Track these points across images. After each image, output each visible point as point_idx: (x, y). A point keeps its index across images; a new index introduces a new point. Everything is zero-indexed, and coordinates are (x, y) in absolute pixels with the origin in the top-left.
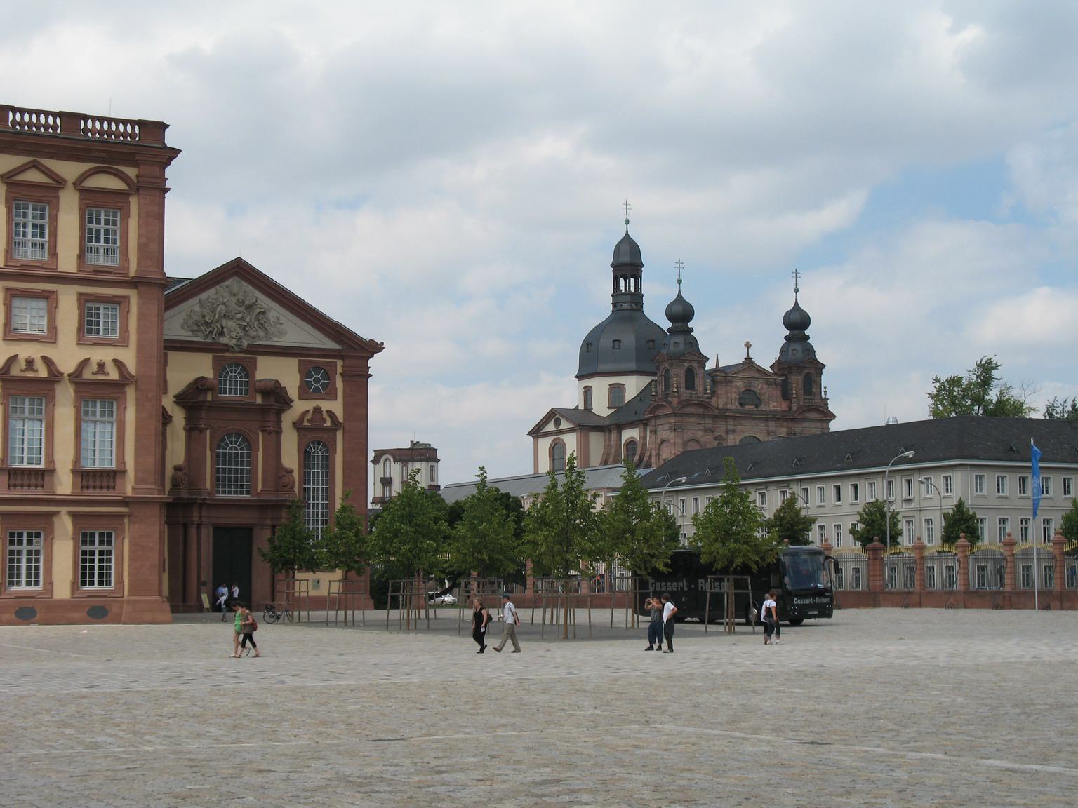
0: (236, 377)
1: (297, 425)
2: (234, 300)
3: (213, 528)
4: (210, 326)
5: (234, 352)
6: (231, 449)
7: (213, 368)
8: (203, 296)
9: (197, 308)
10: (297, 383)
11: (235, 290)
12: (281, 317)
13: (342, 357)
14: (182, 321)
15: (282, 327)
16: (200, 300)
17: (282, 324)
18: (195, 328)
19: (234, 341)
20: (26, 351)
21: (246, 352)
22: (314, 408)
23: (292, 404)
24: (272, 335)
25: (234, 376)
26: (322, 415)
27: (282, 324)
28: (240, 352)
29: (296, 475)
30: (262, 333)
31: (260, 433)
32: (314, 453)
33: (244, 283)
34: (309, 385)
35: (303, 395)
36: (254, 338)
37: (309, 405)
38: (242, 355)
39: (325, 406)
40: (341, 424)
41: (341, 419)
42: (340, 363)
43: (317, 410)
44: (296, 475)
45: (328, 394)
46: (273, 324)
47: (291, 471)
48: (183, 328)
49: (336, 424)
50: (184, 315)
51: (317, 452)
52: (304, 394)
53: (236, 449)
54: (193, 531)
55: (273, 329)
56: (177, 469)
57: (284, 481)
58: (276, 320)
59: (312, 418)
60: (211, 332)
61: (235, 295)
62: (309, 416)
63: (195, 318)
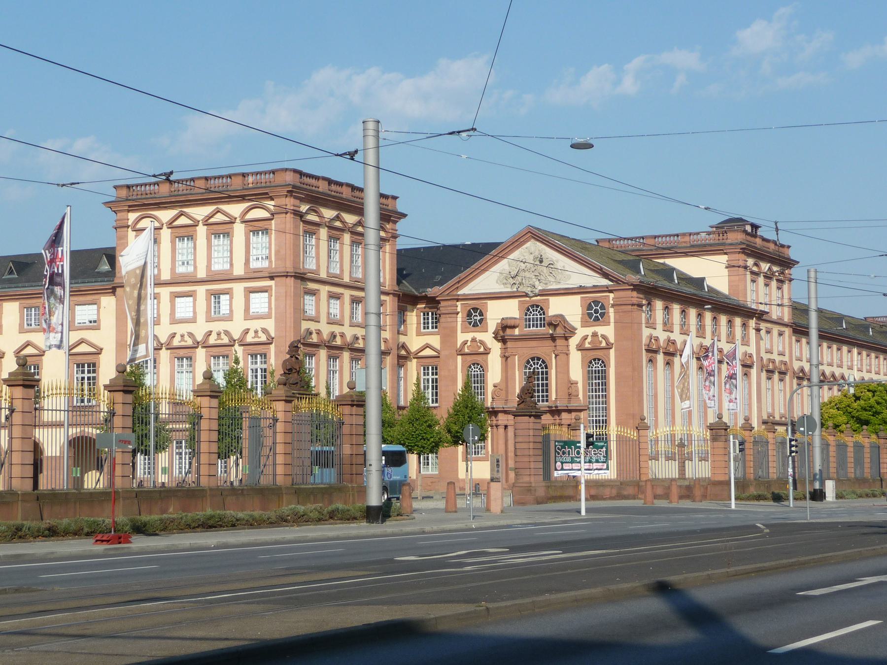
1: (580, 348)
2: (532, 257)
9: (507, 267)
11: (533, 249)
13: (611, 291)
19: (529, 289)
20: (181, 329)
25: (535, 315)
29: (580, 385)
30: (552, 279)
35: (584, 324)
37: (589, 331)
38: (539, 298)
41: (612, 340)
42: (612, 295)
43: (595, 335)
44: (580, 385)
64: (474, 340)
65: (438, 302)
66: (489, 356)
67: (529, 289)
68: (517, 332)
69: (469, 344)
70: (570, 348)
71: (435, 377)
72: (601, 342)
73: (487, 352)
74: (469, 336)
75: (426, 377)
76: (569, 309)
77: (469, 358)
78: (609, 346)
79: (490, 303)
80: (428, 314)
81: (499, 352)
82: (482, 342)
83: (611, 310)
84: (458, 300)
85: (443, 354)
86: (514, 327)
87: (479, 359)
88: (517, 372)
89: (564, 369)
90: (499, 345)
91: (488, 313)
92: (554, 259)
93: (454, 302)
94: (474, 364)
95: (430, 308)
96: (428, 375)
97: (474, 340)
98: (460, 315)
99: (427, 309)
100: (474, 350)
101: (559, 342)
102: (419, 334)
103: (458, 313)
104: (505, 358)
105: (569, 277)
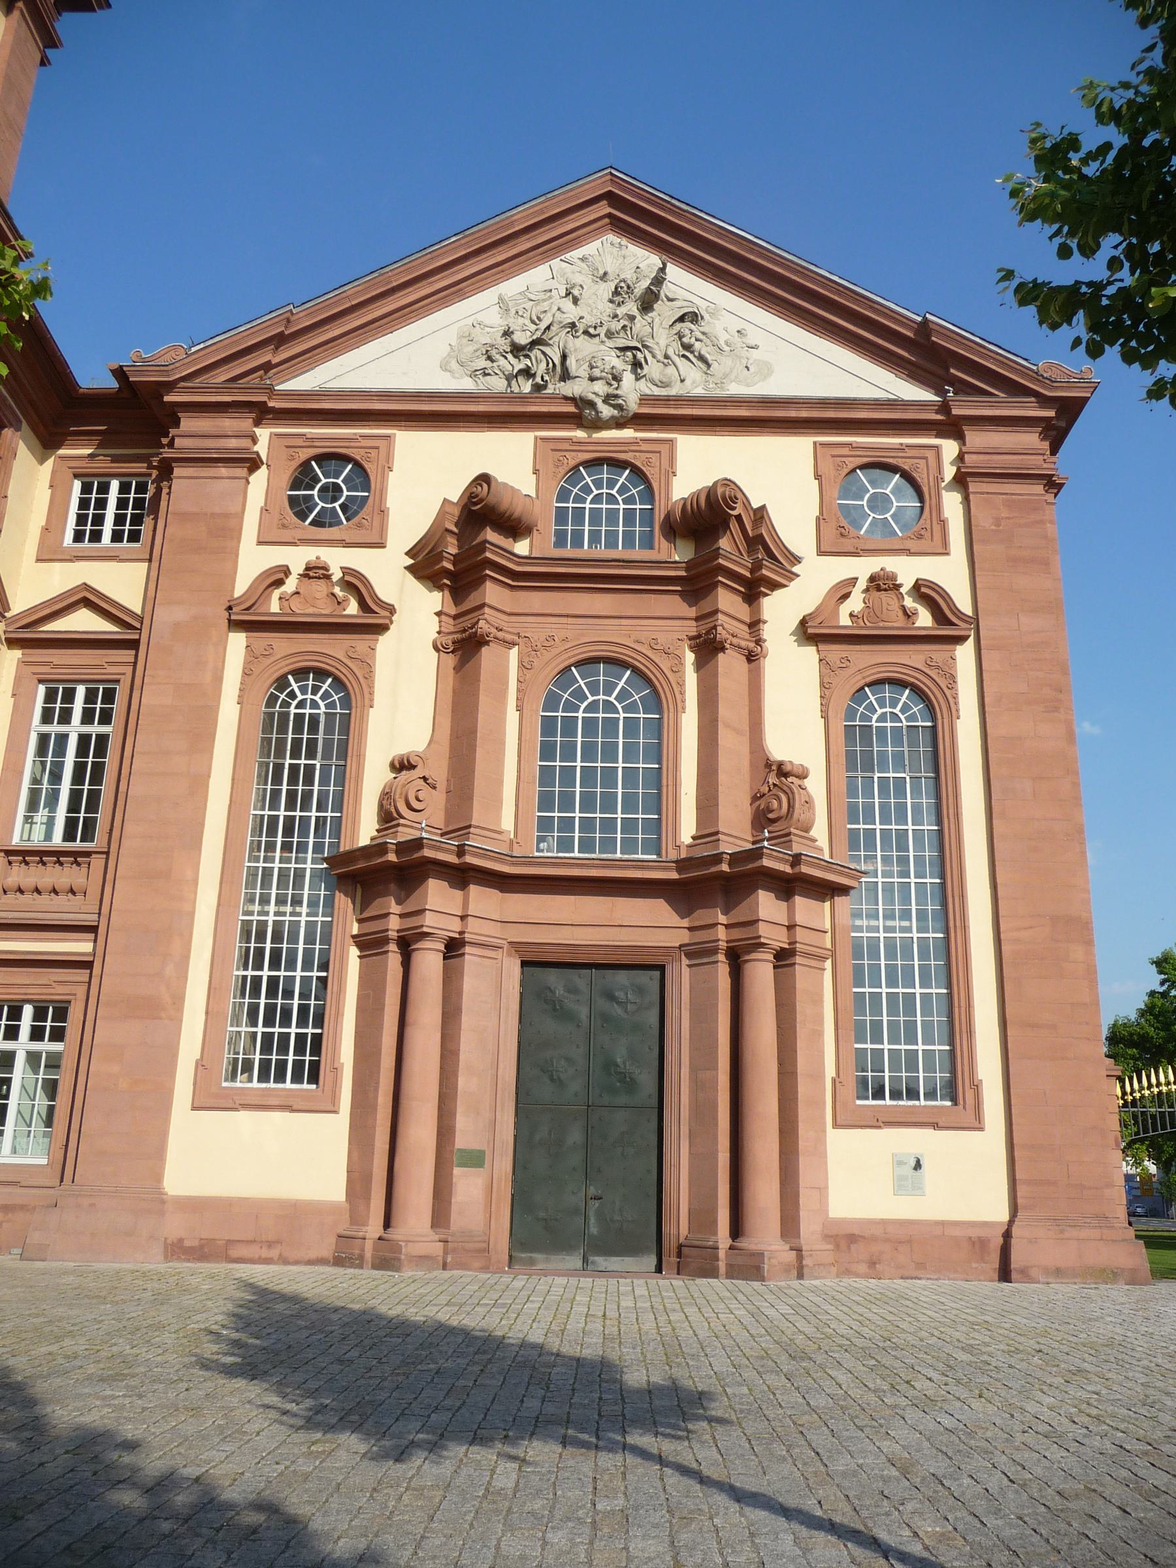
0: (611, 499)
3: (524, 964)
6: (593, 707)
7: (536, 471)
11: (610, 264)
13: (953, 428)
16: (500, 298)
18: (483, 363)
19: (600, 388)
21: (640, 420)
22: (872, 579)
24: (726, 376)
25: (611, 495)
28: (619, 424)
29: (816, 786)
32: (882, 718)
34: (853, 516)
36: (664, 385)
38: (628, 433)
39: (908, 570)
42: (949, 448)
45: (920, 537)
46: (727, 348)
48: (446, 370)
49: (948, 625)
52: (837, 537)
54: (429, 961)
56: (402, 765)
60: (527, 373)
61: (604, 277)
62: (855, 603)
64: (315, 572)
65: (172, 414)
66: (384, 644)
67: (600, 388)
68: (522, 548)
69: (290, 585)
70: (767, 632)
71: (95, 729)
72: (908, 615)
73: (373, 620)
74: (297, 558)
75: (54, 728)
76: (780, 480)
77: (285, 646)
79: (410, 445)
80: (104, 488)
82: (355, 584)
83: (952, 503)
84: (262, 413)
85: (158, 634)
86: (515, 528)
88: (512, 717)
89: (734, 717)
90: (435, 600)
91: (392, 478)
93: (244, 423)
94: (301, 673)
95: (116, 459)
96: (66, 718)
97: (315, 572)
98: (259, 479)
99: (103, 465)
100: (318, 607)
101: (727, 600)
102: (48, 554)
103: (254, 464)
104: (465, 645)
105: (766, 371)
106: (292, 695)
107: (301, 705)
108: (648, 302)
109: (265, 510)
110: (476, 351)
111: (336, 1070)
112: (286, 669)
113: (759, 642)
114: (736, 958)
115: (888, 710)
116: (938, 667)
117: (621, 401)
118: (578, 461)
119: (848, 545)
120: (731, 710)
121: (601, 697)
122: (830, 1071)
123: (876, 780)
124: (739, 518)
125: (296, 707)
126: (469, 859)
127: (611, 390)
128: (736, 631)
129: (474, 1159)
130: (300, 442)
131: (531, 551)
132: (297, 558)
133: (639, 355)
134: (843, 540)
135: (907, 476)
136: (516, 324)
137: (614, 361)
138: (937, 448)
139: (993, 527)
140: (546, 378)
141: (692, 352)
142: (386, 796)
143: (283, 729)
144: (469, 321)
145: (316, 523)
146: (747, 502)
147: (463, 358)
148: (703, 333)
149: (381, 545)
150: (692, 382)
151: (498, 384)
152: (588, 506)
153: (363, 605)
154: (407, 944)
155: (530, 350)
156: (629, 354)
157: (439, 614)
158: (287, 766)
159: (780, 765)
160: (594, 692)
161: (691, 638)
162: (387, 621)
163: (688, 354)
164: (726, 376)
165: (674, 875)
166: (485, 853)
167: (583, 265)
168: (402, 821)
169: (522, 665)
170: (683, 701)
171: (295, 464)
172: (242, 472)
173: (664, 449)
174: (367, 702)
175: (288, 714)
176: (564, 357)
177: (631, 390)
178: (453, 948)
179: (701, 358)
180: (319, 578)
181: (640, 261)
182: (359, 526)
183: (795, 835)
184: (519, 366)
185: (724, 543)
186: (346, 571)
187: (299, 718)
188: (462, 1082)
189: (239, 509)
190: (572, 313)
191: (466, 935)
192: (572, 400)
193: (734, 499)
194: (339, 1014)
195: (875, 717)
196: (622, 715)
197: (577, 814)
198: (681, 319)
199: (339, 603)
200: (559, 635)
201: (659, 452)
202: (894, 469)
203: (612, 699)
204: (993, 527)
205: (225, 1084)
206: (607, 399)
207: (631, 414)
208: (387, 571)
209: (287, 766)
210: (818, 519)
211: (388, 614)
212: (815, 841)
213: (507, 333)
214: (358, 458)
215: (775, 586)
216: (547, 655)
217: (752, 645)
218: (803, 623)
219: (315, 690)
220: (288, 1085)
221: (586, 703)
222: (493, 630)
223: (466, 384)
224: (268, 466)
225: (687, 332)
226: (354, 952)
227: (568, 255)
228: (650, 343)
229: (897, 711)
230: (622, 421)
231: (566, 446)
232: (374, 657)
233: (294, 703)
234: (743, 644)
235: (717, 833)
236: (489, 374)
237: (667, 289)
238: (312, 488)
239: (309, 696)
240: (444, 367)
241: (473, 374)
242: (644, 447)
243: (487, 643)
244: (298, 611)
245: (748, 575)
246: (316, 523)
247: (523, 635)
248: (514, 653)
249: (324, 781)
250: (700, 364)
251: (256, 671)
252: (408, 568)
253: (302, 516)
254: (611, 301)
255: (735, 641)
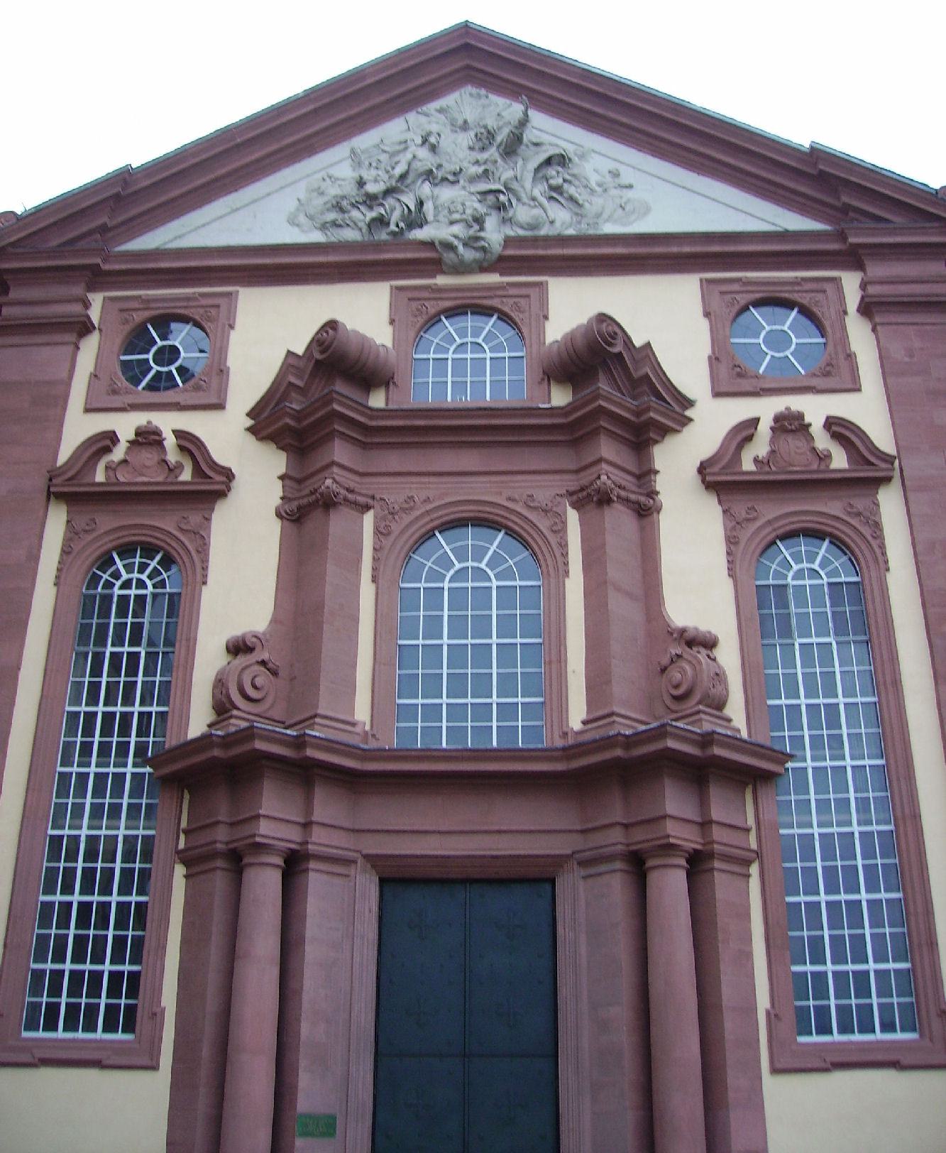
2: (466, 139)
3: (383, 881)
4: (382, 205)
5: (461, 268)
7: (392, 322)
8: (365, 141)
10: (704, 347)
12: (622, 169)
13: (853, 258)
14: (292, 205)
15: (629, 194)
16: (353, 151)
17: (630, 187)
21: (503, 264)
22: (777, 419)
23: (688, 413)
24: (598, 215)
26: (811, 438)
27: (630, 187)
28: (483, 268)
29: (728, 657)
31: (572, 516)
33: (494, 98)
40: (888, 459)
42: (851, 283)
43: (790, 425)
44: (728, 657)
46: (597, 189)
47: (709, 643)
50: (301, 191)
51: (808, 570)
52: (732, 377)
53: (480, 574)
55: (598, 202)
56: (238, 648)
57: (677, 676)
58: (608, 178)
59: (773, 452)
60: (381, 221)
61: (465, 126)
62: (760, 446)
63: (333, 191)
64: (148, 438)
68: (377, 400)
69: (118, 453)
74: (126, 425)
77: (108, 522)
78: (869, 472)
81: (275, 493)
84: (97, 278)
87: (166, 522)
92: (570, 150)
93: (78, 290)
94: (126, 551)
97: (148, 438)
103: (85, 328)
106: (117, 575)
107: (127, 585)
108: (512, 147)
109: (95, 376)
110: (325, 204)
111: (157, 1016)
112: (110, 545)
113: (652, 494)
114: (638, 866)
115: (805, 565)
116: (859, 514)
117: (483, 243)
118: (438, 309)
119: (746, 385)
120: (621, 567)
121: (470, 564)
122: (763, 1001)
123: (797, 647)
124: (619, 356)
125: (122, 587)
126: (310, 752)
127: (471, 232)
128: (624, 483)
129: (326, 1126)
130: (135, 305)
131: (387, 404)
132: (126, 425)
133: (502, 198)
134: (739, 380)
135: (806, 312)
136: (368, 175)
137: (474, 206)
138: (836, 281)
139: (907, 359)
140: (402, 225)
141: (561, 194)
142: (220, 683)
143: (105, 613)
144: (319, 176)
145: (151, 387)
146: (628, 341)
147: (311, 211)
148: (574, 175)
149: (220, 406)
150: (561, 220)
151: (350, 235)
152: (450, 355)
153: (197, 470)
154: (237, 860)
155: (384, 198)
156: (491, 198)
157: (282, 478)
158: (108, 655)
159: (683, 631)
160: (462, 557)
161: (571, 494)
162: (223, 487)
163: (555, 195)
164: (598, 215)
165: (560, 767)
166: (329, 745)
167: (442, 117)
168: (235, 712)
169: (378, 532)
170: (566, 564)
171: (128, 328)
172: (71, 337)
173: (533, 293)
174: (199, 578)
175: (111, 596)
176: (421, 204)
177: (494, 234)
178: (294, 865)
179: (571, 199)
180: (150, 444)
181: (503, 111)
182: (197, 388)
183: (705, 713)
184: (371, 215)
185: (604, 385)
186: (179, 434)
187: (124, 600)
188: (305, 1029)
189: (65, 375)
190: (425, 159)
191: (310, 847)
192: (430, 245)
193: (614, 336)
194: (162, 948)
195: (790, 575)
196: (495, 583)
197: (445, 700)
198: (548, 162)
199: (170, 470)
200: (419, 496)
201: (528, 296)
202: (788, 304)
203: (483, 566)
204: (907, 359)
205: (25, 1034)
206: (470, 242)
207: (494, 257)
208: (225, 434)
209: (108, 655)
210: (710, 358)
211: (224, 479)
212: (729, 720)
213: (361, 183)
214: (197, 317)
215: (665, 431)
216: (407, 519)
217: (642, 499)
218: (702, 469)
219: (143, 567)
220: (99, 1034)
221: (452, 572)
222: (343, 492)
223: (317, 237)
224: (100, 330)
225: (554, 173)
226: (180, 870)
227: (424, 108)
228: (515, 185)
229: (816, 566)
230: (485, 264)
231: (426, 294)
232: (209, 528)
233: (118, 583)
234: (633, 497)
235: (612, 714)
236: (340, 226)
237: (529, 135)
238: (147, 352)
239: (136, 575)
240: (292, 221)
241: (323, 227)
242: (512, 291)
243: (335, 505)
244: (122, 479)
245: (633, 418)
246: (151, 387)
247: (378, 497)
248: (368, 519)
249: (149, 671)
250: (571, 205)
251: (77, 547)
252: (249, 429)
253: (136, 382)
254: (471, 149)
255: (623, 493)
